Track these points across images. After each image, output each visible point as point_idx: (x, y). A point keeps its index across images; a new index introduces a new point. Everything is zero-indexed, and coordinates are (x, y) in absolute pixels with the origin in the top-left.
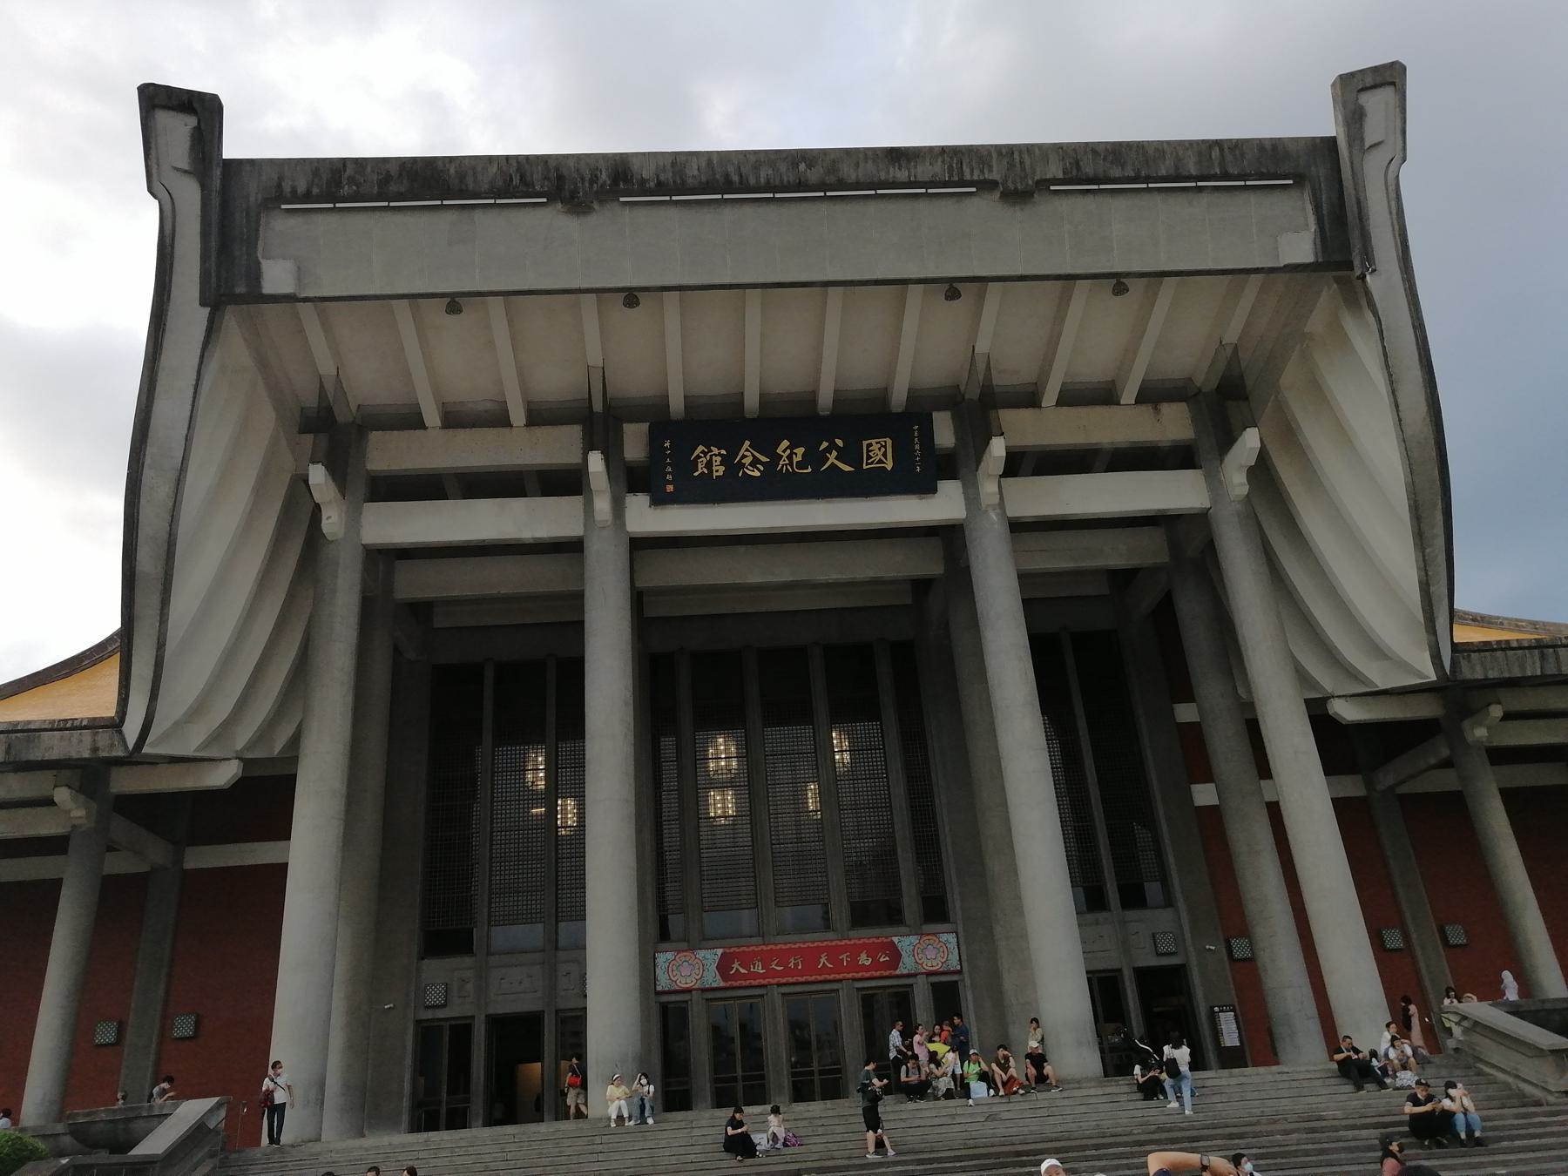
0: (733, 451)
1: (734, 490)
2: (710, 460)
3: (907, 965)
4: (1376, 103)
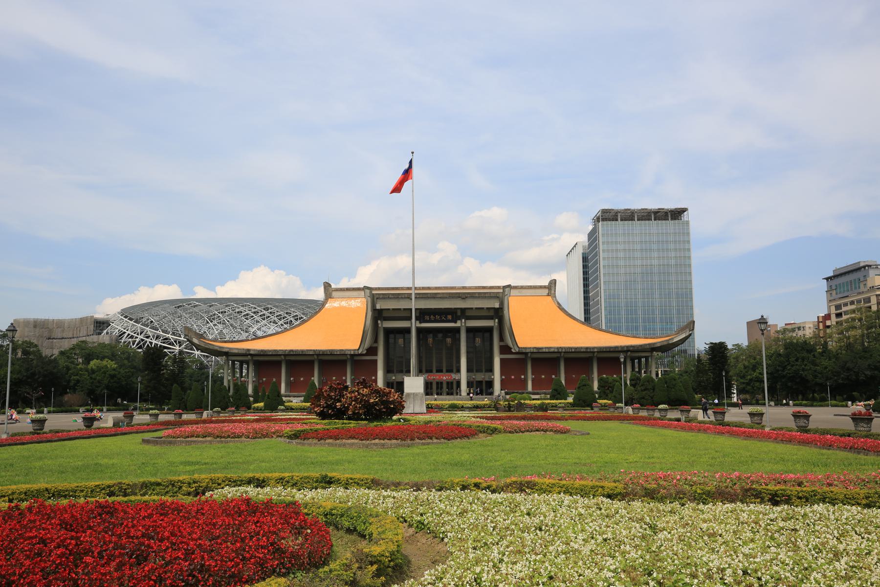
0: (430, 316)
1: (430, 321)
2: (427, 318)
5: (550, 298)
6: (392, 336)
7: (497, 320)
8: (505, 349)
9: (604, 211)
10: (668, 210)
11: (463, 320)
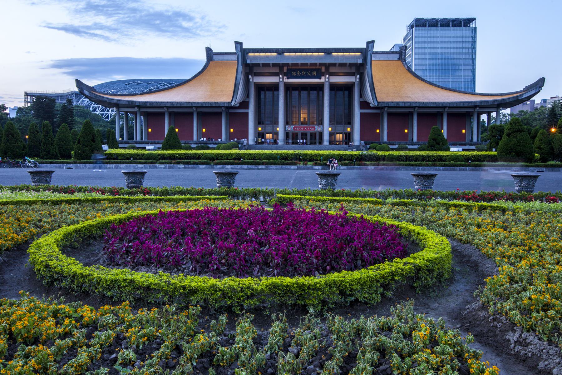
2: (294, 73)
3: (316, 130)
4: (370, 45)
5: (400, 62)
6: (263, 92)
7: (358, 76)
8: (364, 104)
9: (417, 20)
10: (462, 19)
11: (327, 76)
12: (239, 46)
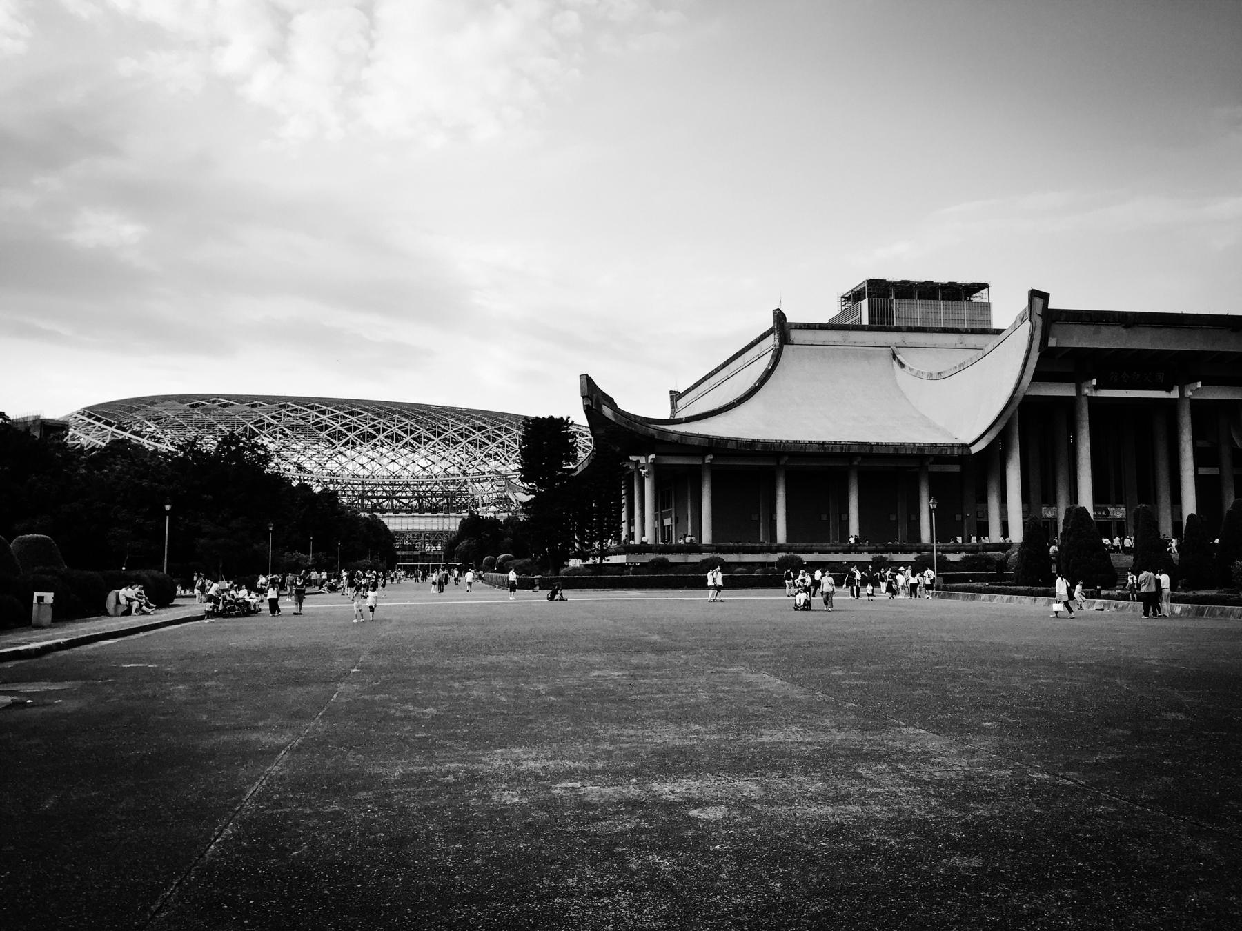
9: (873, 283)
12: (1039, 302)
